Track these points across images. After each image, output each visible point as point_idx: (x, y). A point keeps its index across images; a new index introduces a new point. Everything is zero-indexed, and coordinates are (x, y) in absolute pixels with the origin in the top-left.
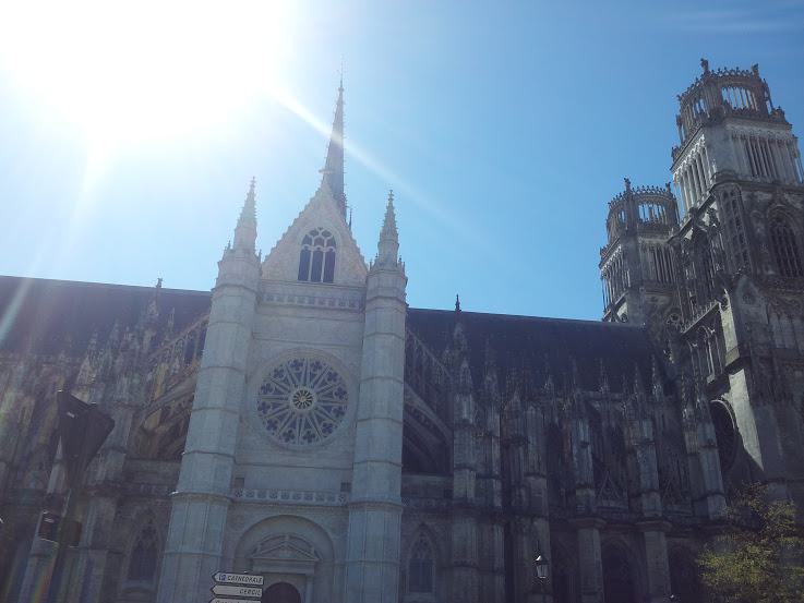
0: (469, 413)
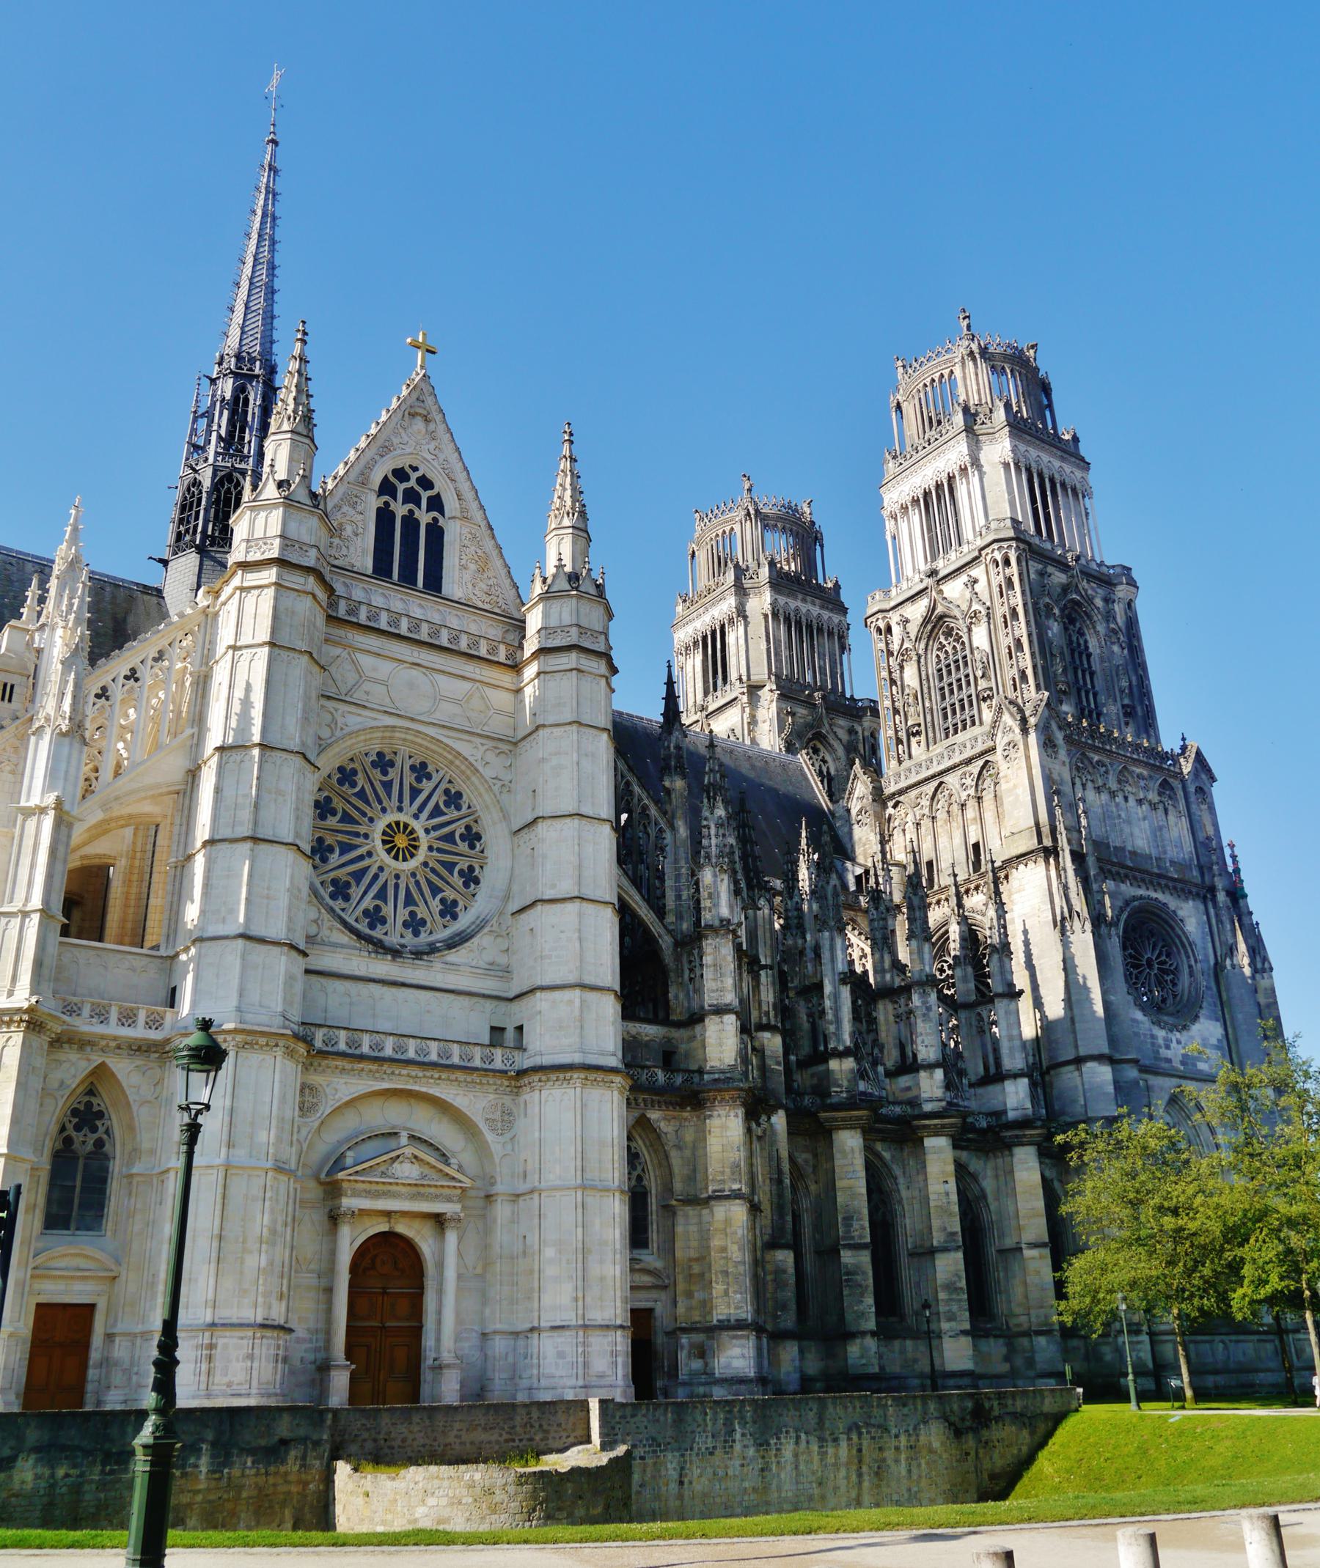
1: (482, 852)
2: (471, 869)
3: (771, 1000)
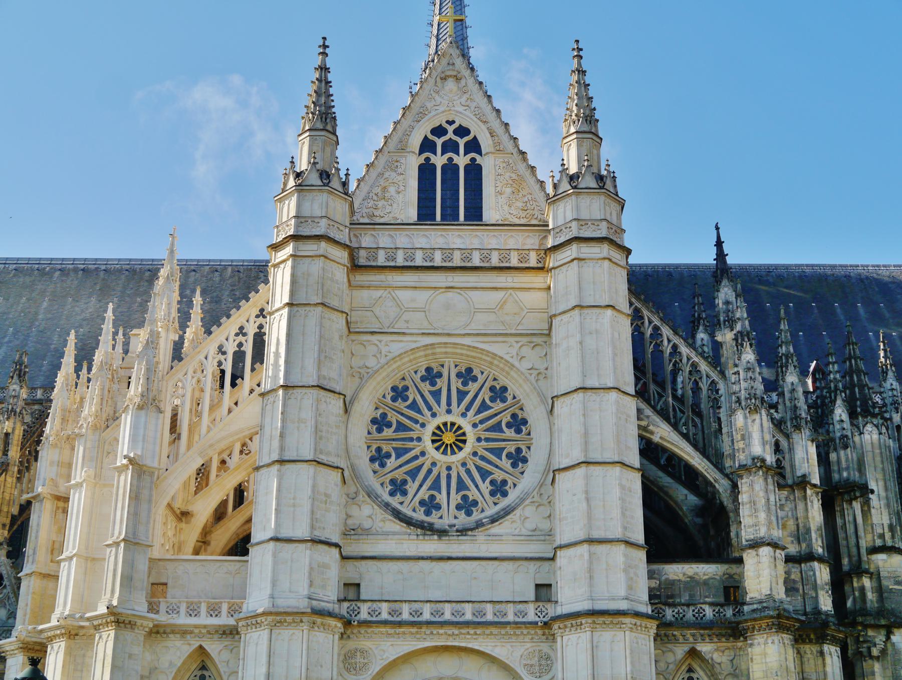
0: (764, 443)
1: (529, 434)
2: (519, 450)
3: (886, 521)
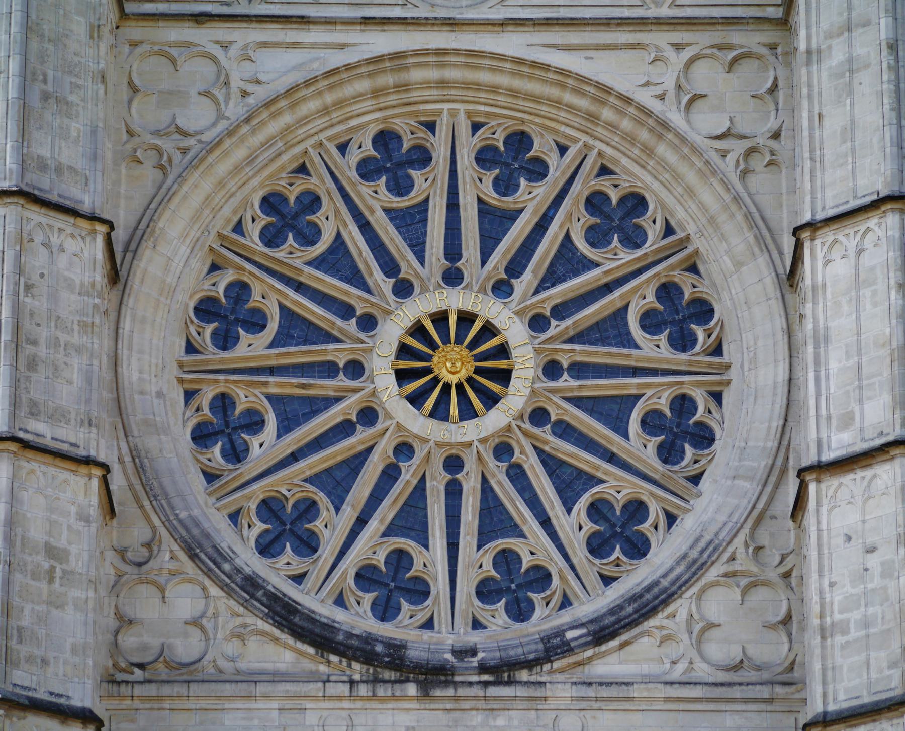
1: (718, 351)
2: (683, 404)
